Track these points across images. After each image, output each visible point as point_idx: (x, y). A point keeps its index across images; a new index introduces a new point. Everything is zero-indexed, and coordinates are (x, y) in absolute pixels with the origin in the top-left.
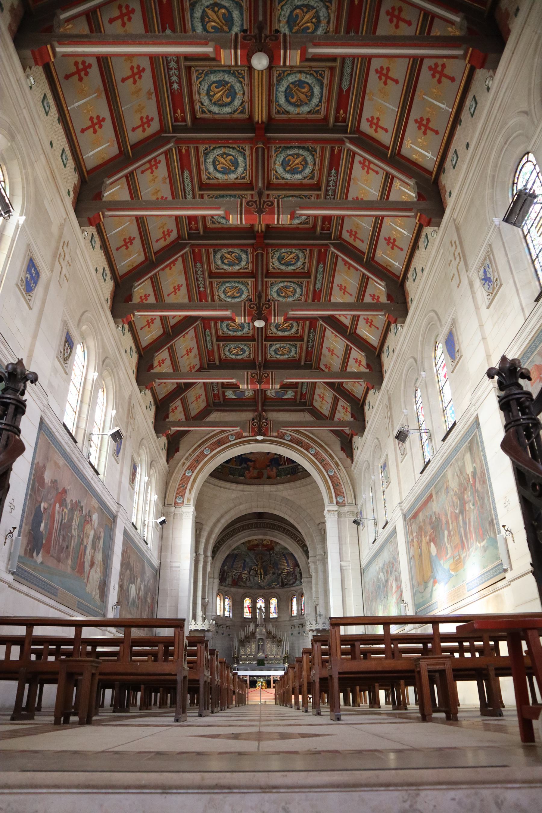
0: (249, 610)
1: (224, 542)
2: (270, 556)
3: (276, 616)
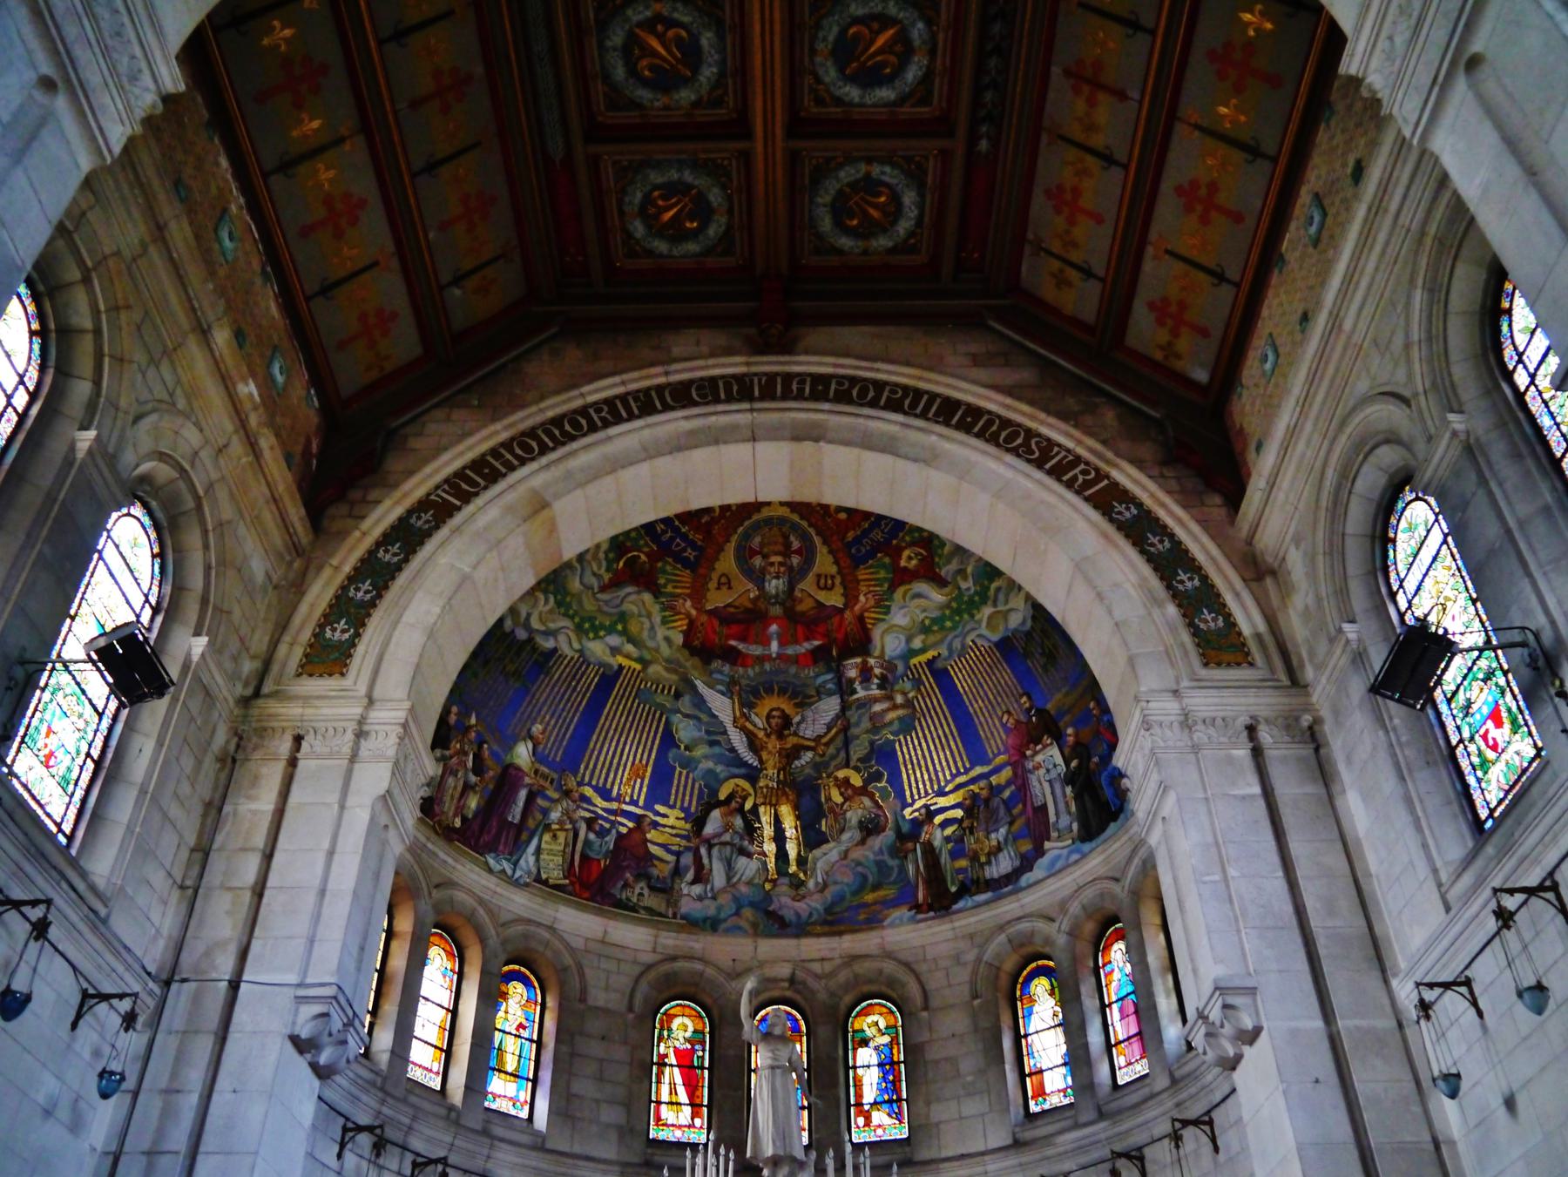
0: (692, 1086)
1: (494, 477)
2: (844, 707)
3: (902, 1132)
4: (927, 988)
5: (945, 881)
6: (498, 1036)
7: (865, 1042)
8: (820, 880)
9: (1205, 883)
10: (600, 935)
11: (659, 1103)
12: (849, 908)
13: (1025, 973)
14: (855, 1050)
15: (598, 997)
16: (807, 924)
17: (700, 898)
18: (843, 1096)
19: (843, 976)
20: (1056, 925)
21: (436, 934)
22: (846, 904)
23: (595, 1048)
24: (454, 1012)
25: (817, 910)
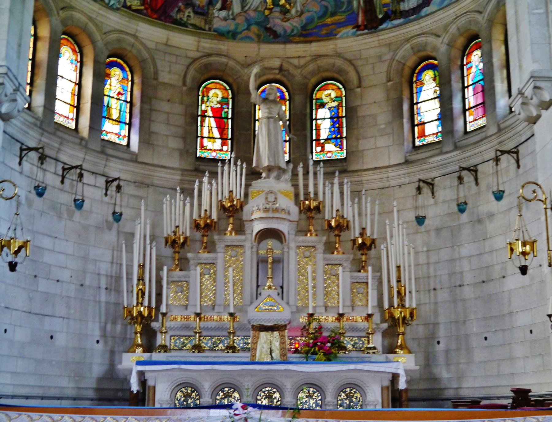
0: (221, 128)
3: (343, 155)
4: (361, 75)
5: (375, 11)
6: (106, 99)
7: (323, 105)
8: (299, 9)
9: (534, 14)
10: (164, 41)
11: (202, 137)
12: (316, 27)
13: (420, 67)
14: (317, 109)
15: (165, 77)
16: (290, 36)
17: (225, 19)
18: (309, 135)
19: (311, 67)
20: (441, 39)
21: (64, 38)
22: (313, 25)
23: (165, 107)
24: (79, 85)
25: (296, 27)
